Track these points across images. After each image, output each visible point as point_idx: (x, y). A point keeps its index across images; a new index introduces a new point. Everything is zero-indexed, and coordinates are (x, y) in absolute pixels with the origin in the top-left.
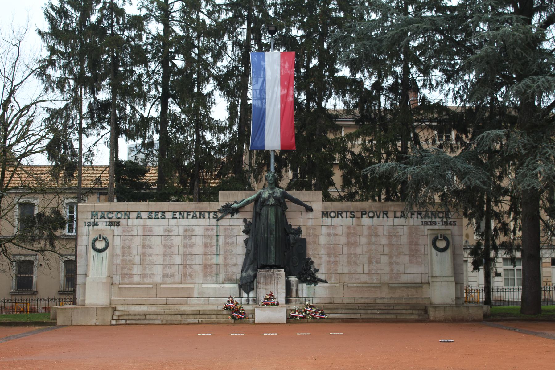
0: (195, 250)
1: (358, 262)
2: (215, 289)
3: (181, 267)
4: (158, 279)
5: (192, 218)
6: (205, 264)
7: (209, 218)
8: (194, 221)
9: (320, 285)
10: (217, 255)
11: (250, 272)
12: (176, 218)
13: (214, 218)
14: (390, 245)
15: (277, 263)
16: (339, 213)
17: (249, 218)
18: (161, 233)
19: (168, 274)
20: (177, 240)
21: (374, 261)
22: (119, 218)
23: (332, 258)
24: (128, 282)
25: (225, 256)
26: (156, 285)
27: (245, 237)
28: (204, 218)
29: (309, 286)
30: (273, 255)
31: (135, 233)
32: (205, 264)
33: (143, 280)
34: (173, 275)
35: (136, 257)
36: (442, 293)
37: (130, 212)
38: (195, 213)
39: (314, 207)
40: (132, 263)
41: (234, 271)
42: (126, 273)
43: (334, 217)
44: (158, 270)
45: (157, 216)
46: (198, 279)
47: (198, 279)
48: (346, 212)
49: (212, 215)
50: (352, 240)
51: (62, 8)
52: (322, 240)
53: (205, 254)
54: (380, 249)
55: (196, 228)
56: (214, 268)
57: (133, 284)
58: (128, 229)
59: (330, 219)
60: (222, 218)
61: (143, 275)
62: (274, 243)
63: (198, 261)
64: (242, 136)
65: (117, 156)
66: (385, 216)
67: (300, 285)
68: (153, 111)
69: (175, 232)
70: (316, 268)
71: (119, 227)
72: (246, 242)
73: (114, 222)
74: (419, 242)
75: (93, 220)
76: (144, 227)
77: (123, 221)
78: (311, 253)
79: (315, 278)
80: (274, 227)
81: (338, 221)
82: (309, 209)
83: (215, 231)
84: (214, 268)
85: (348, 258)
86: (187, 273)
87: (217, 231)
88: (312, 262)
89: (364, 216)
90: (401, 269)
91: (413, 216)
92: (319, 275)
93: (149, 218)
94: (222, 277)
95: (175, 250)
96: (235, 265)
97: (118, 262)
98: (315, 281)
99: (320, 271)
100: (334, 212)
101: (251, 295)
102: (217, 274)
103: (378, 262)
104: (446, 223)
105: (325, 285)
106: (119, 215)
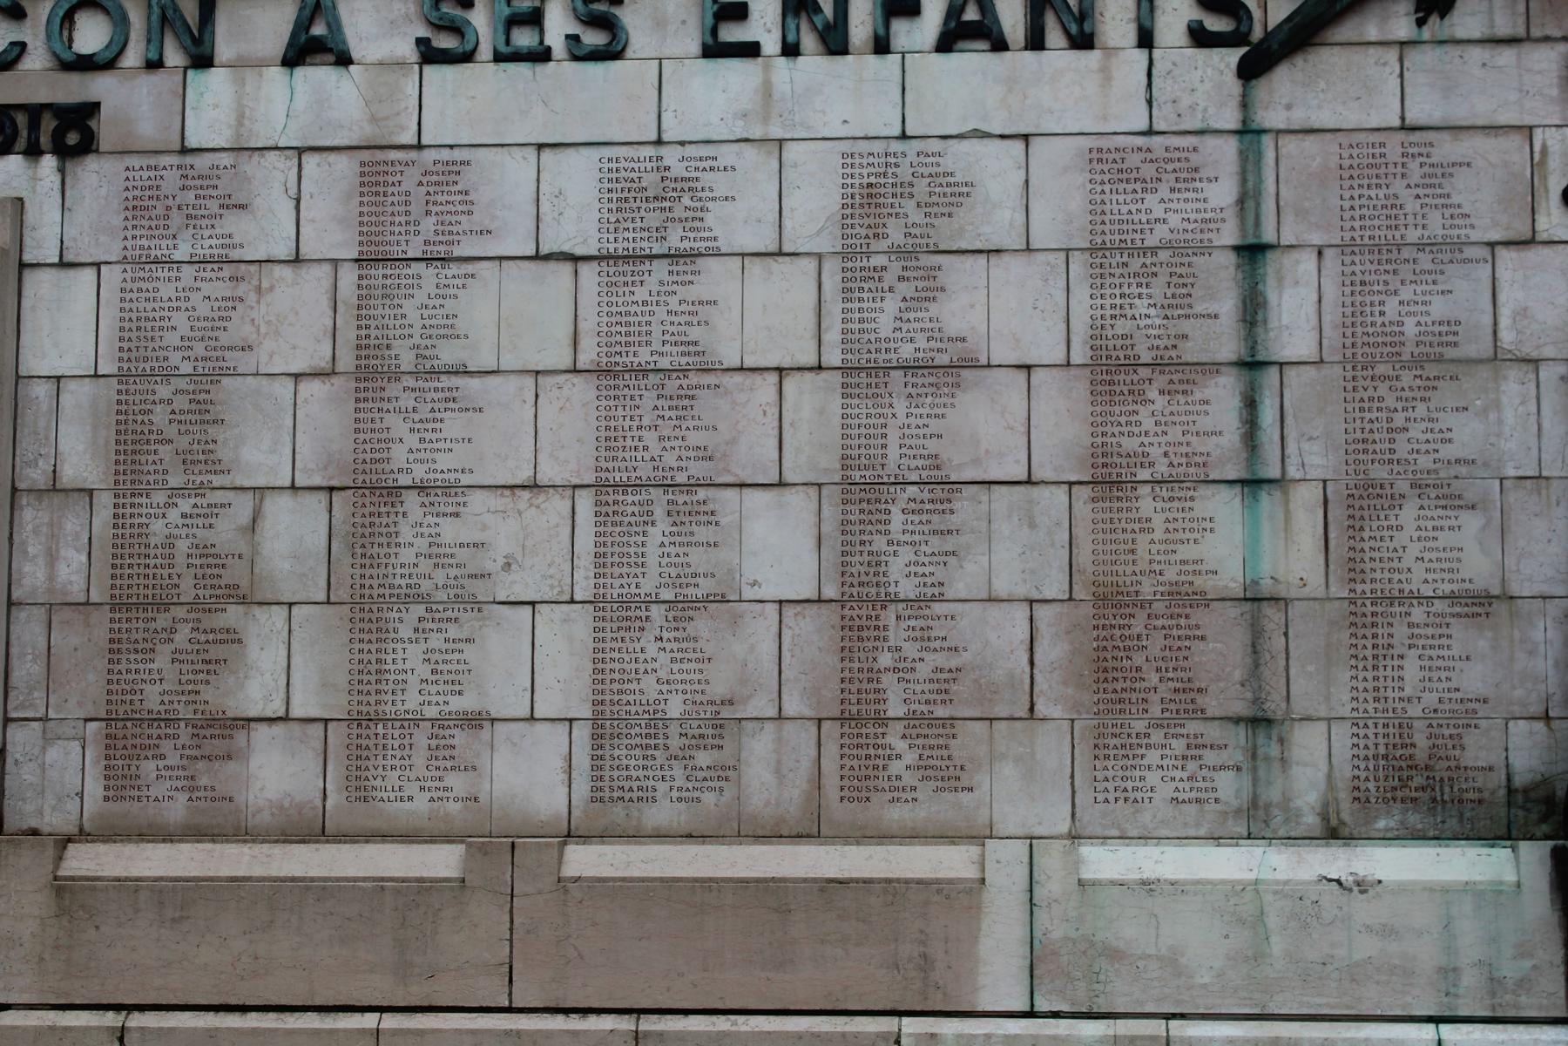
0: (982, 428)
2: (1245, 906)
3: (812, 635)
4: (532, 776)
5: (945, 44)
7: (1146, 39)
8: (962, 86)
10: (1252, 484)
12: (750, 50)
13: (1200, 37)
18: (577, 227)
19: (656, 721)
20: (766, 315)
22: (86, 64)
24: (177, 810)
25: (1360, 503)
26: (502, 845)
28: (1083, 41)
31: (265, 230)
33: (360, 790)
34: (718, 724)
35: (280, 510)
40: (230, 588)
41: (1474, 680)
42: (153, 698)
44: (531, 670)
45: (524, 38)
46: (1026, 785)
47: (1026, 785)
53: (1108, 480)
56: (1219, 651)
57: (244, 834)
58: (193, 183)
61: (363, 727)
63: (1007, 571)
69: (739, 221)
73: (35, 112)
76: (377, 161)
77: (129, 101)
83: (1222, 193)
84: (1219, 651)
86: (884, 715)
87: (1247, 199)
93: (430, 55)
94: (1315, 761)
95: (744, 424)
96: (1480, 604)
97: (71, 571)
102: (1259, 722)
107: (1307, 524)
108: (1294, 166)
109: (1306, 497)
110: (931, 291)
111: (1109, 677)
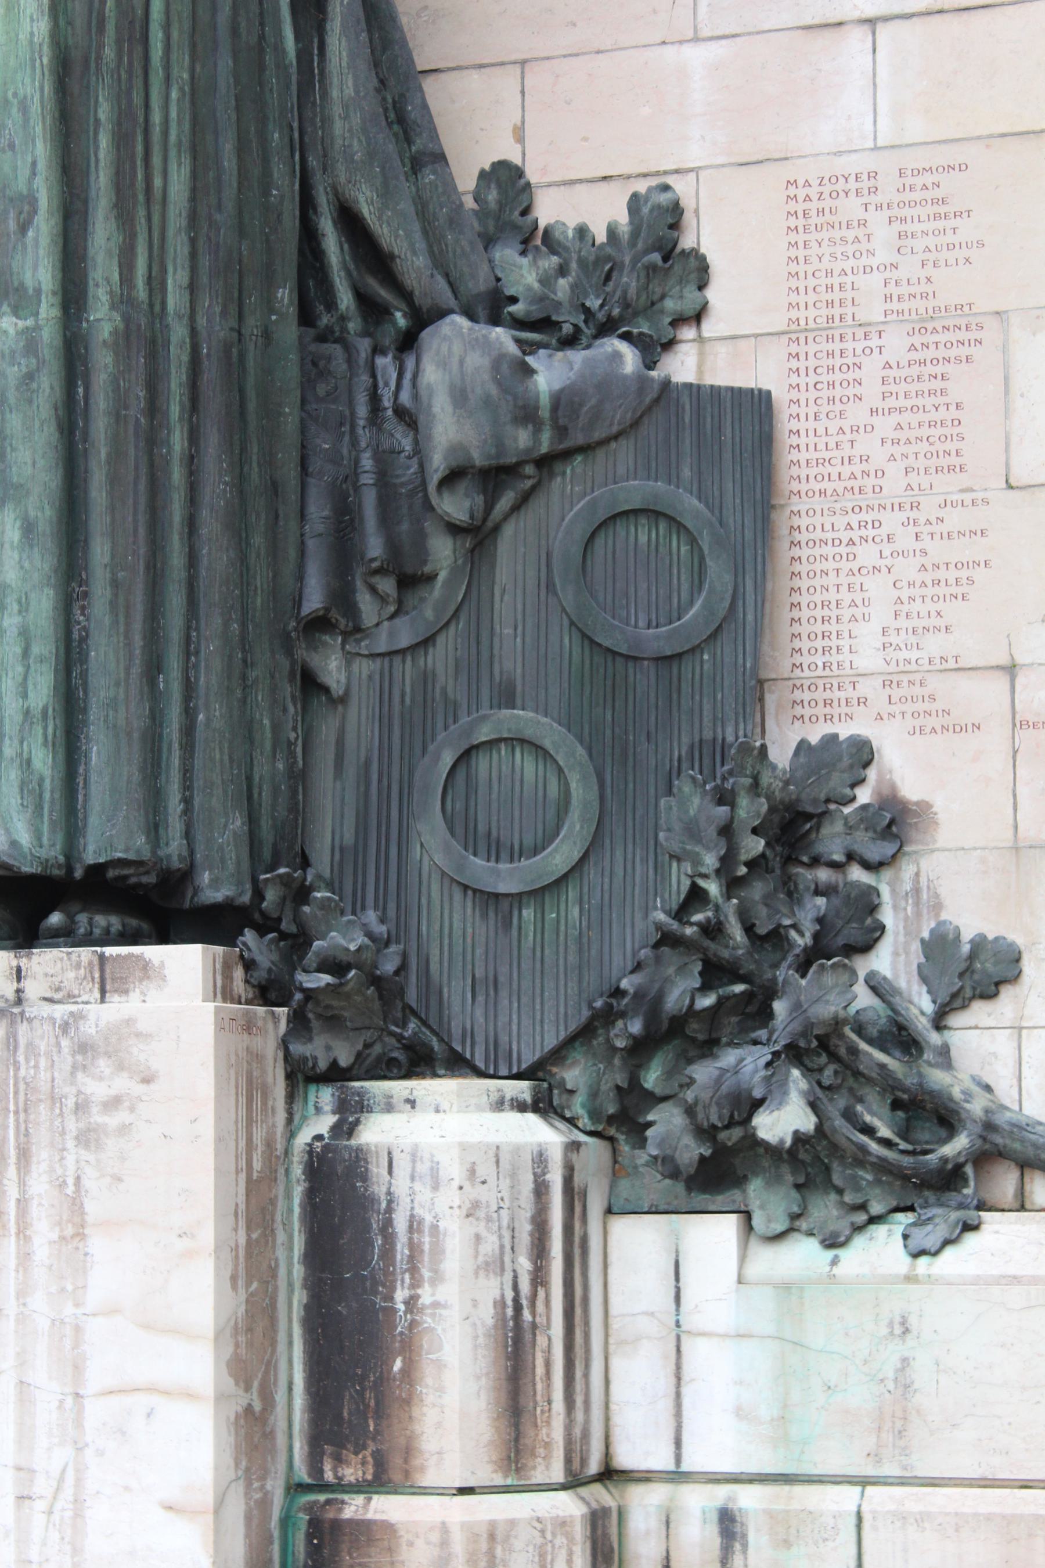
15: (110, 836)
29: (803, 1254)
70: (971, 919)
78: (865, 651)
88: (895, 825)
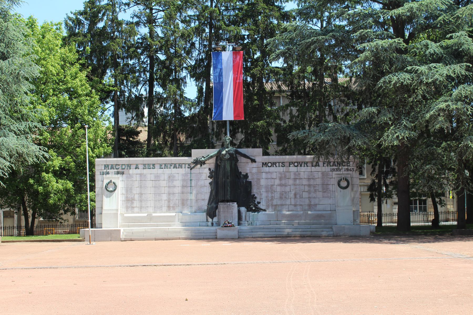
1: (287, 197)
3: (166, 202)
6: (183, 200)
9: (261, 213)
11: (214, 205)
13: (188, 168)
14: (309, 186)
16: (274, 164)
17: (213, 167)
18: (153, 179)
21: (298, 196)
23: (270, 195)
27: (210, 180)
30: (229, 193)
32: (183, 200)
36: (344, 218)
37: (130, 165)
38: (175, 164)
39: (257, 159)
43: (271, 166)
48: (279, 163)
49: (187, 166)
50: (283, 182)
51: (77, 19)
52: (263, 182)
53: (183, 193)
54: (302, 188)
55: (177, 175)
59: (268, 168)
60: (194, 167)
62: (229, 185)
64: (207, 110)
65: (118, 123)
66: (305, 165)
67: (248, 212)
68: (143, 91)
69: (162, 178)
71: (124, 175)
72: (210, 184)
74: (329, 183)
75: (105, 171)
76: (141, 175)
77: (125, 171)
79: (258, 208)
80: (229, 174)
81: (273, 169)
82: (253, 161)
83: (189, 177)
85: (280, 194)
87: (191, 177)
88: (256, 198)
89: (291, 165)
90: (317, 201)
91: (325, 165)
92: (261, 206)
96: (203, 200)
98: (258, 210)
99: (261, 203)
100: (270, 163)
101: (215, 219)
103: (301, 197)
104: (348, 170)
105: (264, 212)
106: (124, 167)
107: (194, 195)
108: (193, 175)
109: (194, 194)
110: (173, 182)
111: (183, 204)
